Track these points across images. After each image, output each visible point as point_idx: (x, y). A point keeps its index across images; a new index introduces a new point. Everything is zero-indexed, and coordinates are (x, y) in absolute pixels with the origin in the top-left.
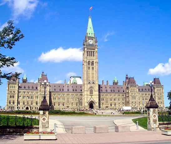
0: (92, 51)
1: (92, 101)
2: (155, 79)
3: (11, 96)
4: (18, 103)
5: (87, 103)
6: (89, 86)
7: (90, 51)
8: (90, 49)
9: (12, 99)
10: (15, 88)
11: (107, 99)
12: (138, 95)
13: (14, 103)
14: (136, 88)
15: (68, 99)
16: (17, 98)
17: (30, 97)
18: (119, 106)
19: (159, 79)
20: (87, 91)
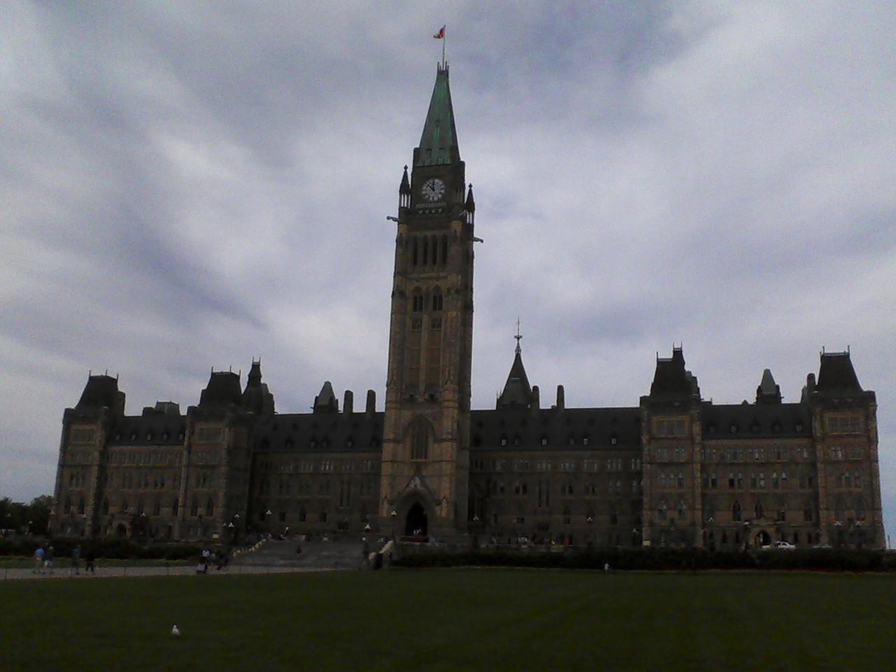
0: (434, 236)
1: (415, 494)
4: (101, 503)
5: (391, 503)
6: (407, 414)
7: (426, 237)
12: (698, 457)
16: (93, 481)
20: (395, 441)
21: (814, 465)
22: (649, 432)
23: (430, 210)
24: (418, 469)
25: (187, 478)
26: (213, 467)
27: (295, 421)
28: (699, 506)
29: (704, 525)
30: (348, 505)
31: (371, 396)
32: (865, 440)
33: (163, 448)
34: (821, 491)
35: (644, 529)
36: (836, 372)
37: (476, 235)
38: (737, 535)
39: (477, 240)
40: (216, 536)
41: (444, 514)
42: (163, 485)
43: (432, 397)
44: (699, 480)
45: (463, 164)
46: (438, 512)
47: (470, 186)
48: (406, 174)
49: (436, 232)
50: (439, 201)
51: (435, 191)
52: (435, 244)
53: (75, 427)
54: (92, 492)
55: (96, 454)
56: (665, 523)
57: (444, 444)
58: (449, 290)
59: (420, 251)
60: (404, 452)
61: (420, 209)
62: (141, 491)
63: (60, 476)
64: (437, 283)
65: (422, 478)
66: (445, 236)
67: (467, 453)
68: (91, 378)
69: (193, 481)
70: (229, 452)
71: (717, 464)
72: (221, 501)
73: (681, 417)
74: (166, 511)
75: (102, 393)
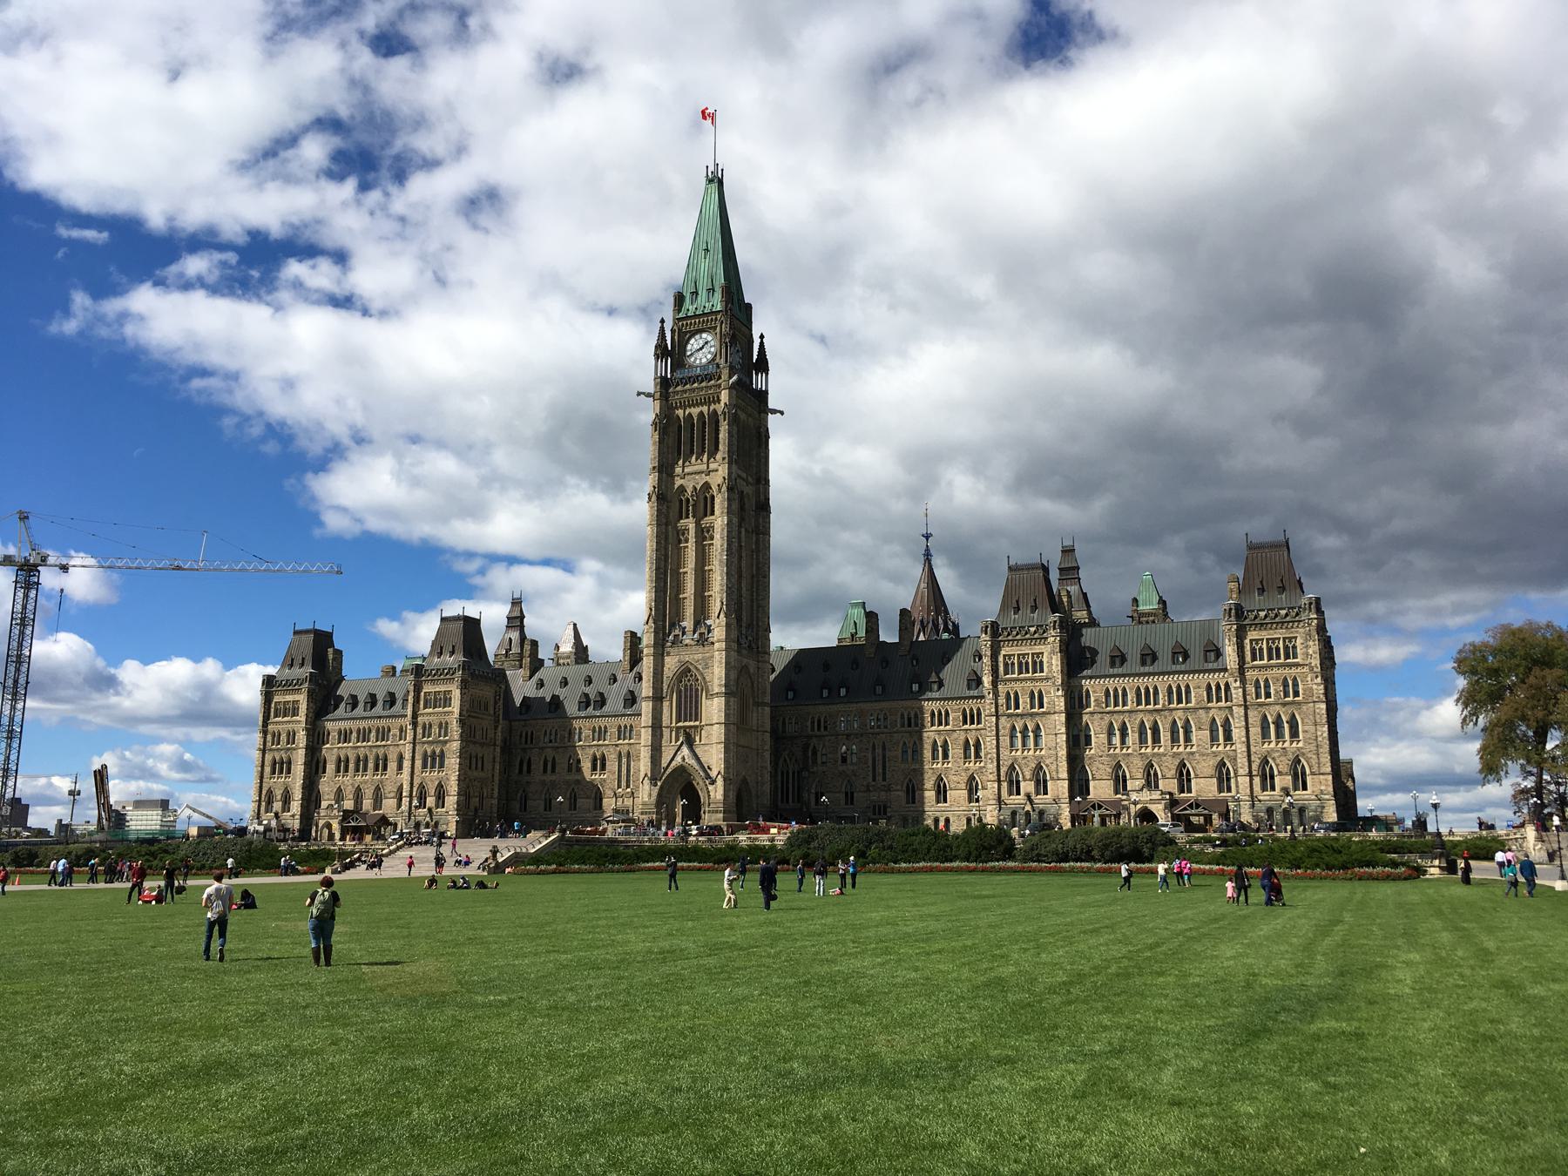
1: (682, 770)
6: (671, 663)
9: (277, 783)
11: (879, 751)
13: (287, 800)
14: (1045, 649)
15: (624, 760)
16: (299, 769)
17: (371, 765)
28: (1065, 775)
37: (771, 406)
39: (774, 412)
42: (385, 768)
44: (1064, 737)
45: (749, 306)
47: (762, 337)
48: (662, 330)
49: (705, 409)
51: (703, 349)
67: (767, 709)
68: (296, 633)
69: (418, 763)
70: (462, 722)
72: (453, 787)
73: (1037, 649)
74: (389, 805)
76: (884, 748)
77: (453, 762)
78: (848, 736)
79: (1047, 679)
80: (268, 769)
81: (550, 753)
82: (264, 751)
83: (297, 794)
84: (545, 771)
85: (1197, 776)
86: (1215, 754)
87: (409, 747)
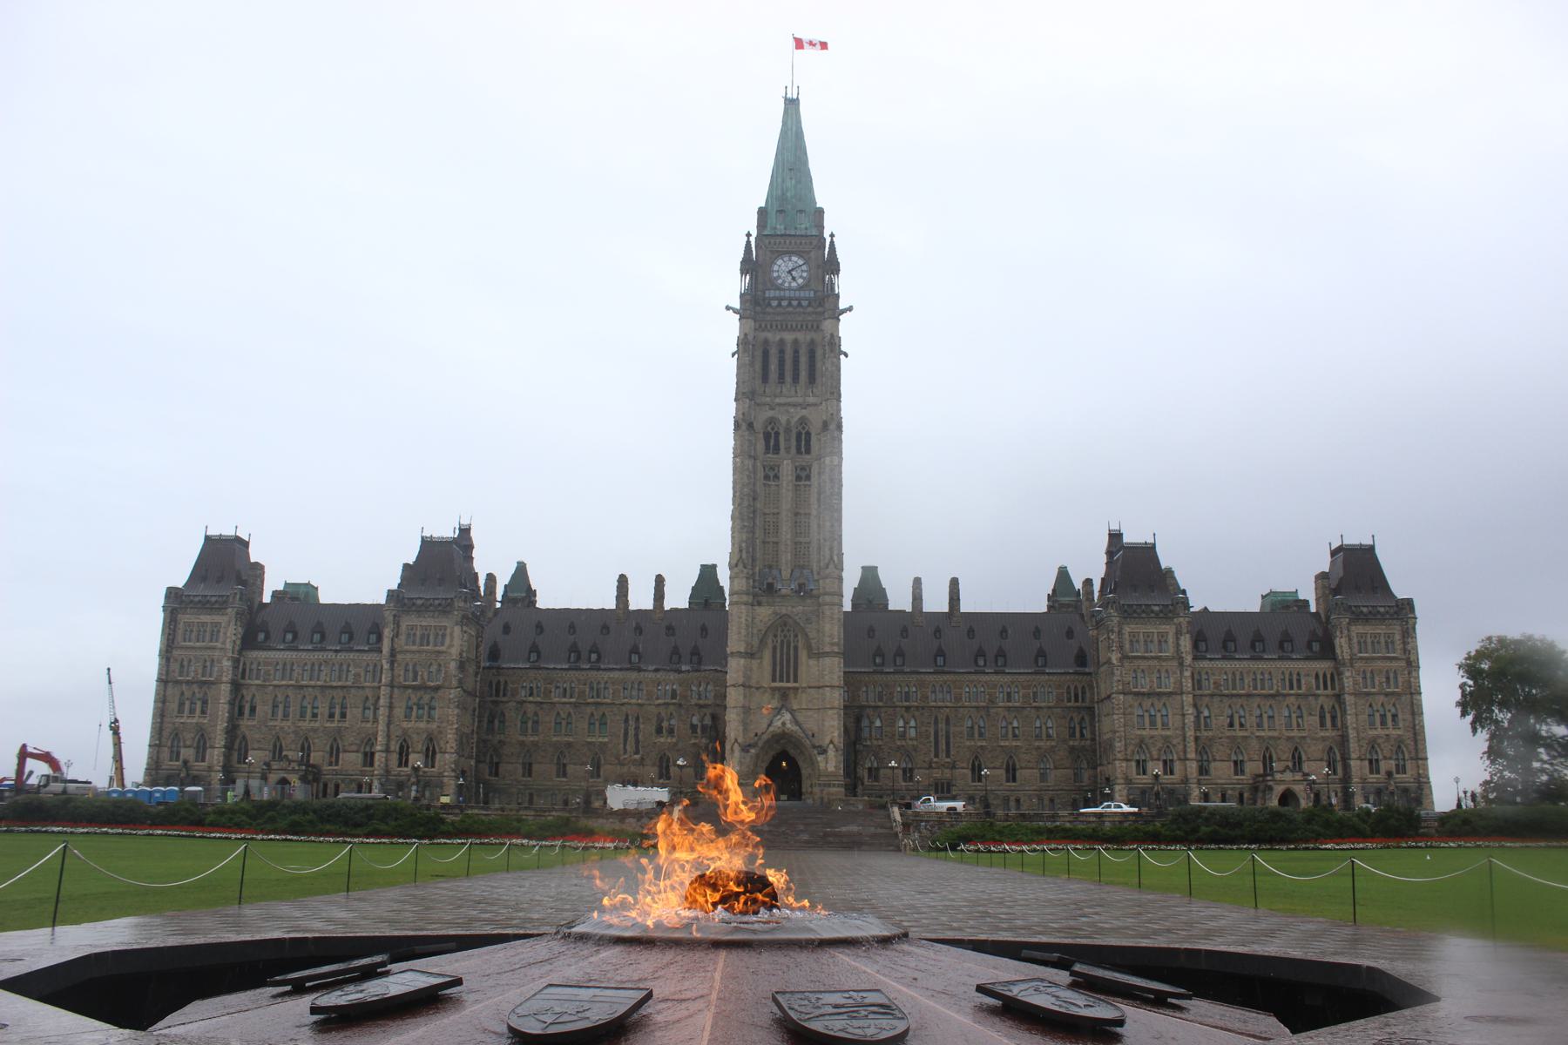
0: (796, 341)
1: (782, 736)
2: (1340, 549)
3: (188, 694)
4: (236, 745)
6: (765, 613)
7: (782, 341)
8: (785, 328)
10: (214, 635)
11: (942, 726)
13: (202, 748)
14: (1170, 630)
16: (222, 710)
17: (323, 709)
18: (1043, 777)
19: (1371, 548)
20: (750, 655)
21: (1339, 697)
22: (1121, 647)
23: (790, 299)
24: (784, 695)
25: (391, 707)
26: (437, 688)
27: (572, 620)
28: (1192, 755)
29: (1199, 783)
30: (637, 752)
31: (660, 581)
32: (1403, 664)
33: (342, 656)
34: (1352, 734)
35: (1117, 788)
36: (1356, 571)
38: (1241, 795)
40: (445, 800)
41: (831, 768)
42: (343, 715)
43: (801, 586)
46: (822, 765)
49: (800, 336)
50: (801, 288)
52: (796, 352)
53: (184, 618)
54: (222, 725)
55: (227, 664)
56: (1146, 779)
57: (827, 661)
58: (825, 425)
59: (773, 367)
60: (762, 671)
61: (774, 298)
62: (305, 725)
63: (162, 701)
64: (804, 412)
65: (792, 712)
66: (812, 342)
68: (207, 538)
69: (399, 712)
70: (462, 666)
71: (1212, 695)
72: (450, 740)
73: (1164, 628)
75: (224, 562)
76: (948, 719)
77: (453, 712)
78: (908, 708)
79: (1173, 658)
80: (173, 706)
81: (531, 709)
82: (164, 681)
83: (220, 740)
84: (524, 732)
85: (1309, 760)
86: (1324, 739)
87: (384, 691)
